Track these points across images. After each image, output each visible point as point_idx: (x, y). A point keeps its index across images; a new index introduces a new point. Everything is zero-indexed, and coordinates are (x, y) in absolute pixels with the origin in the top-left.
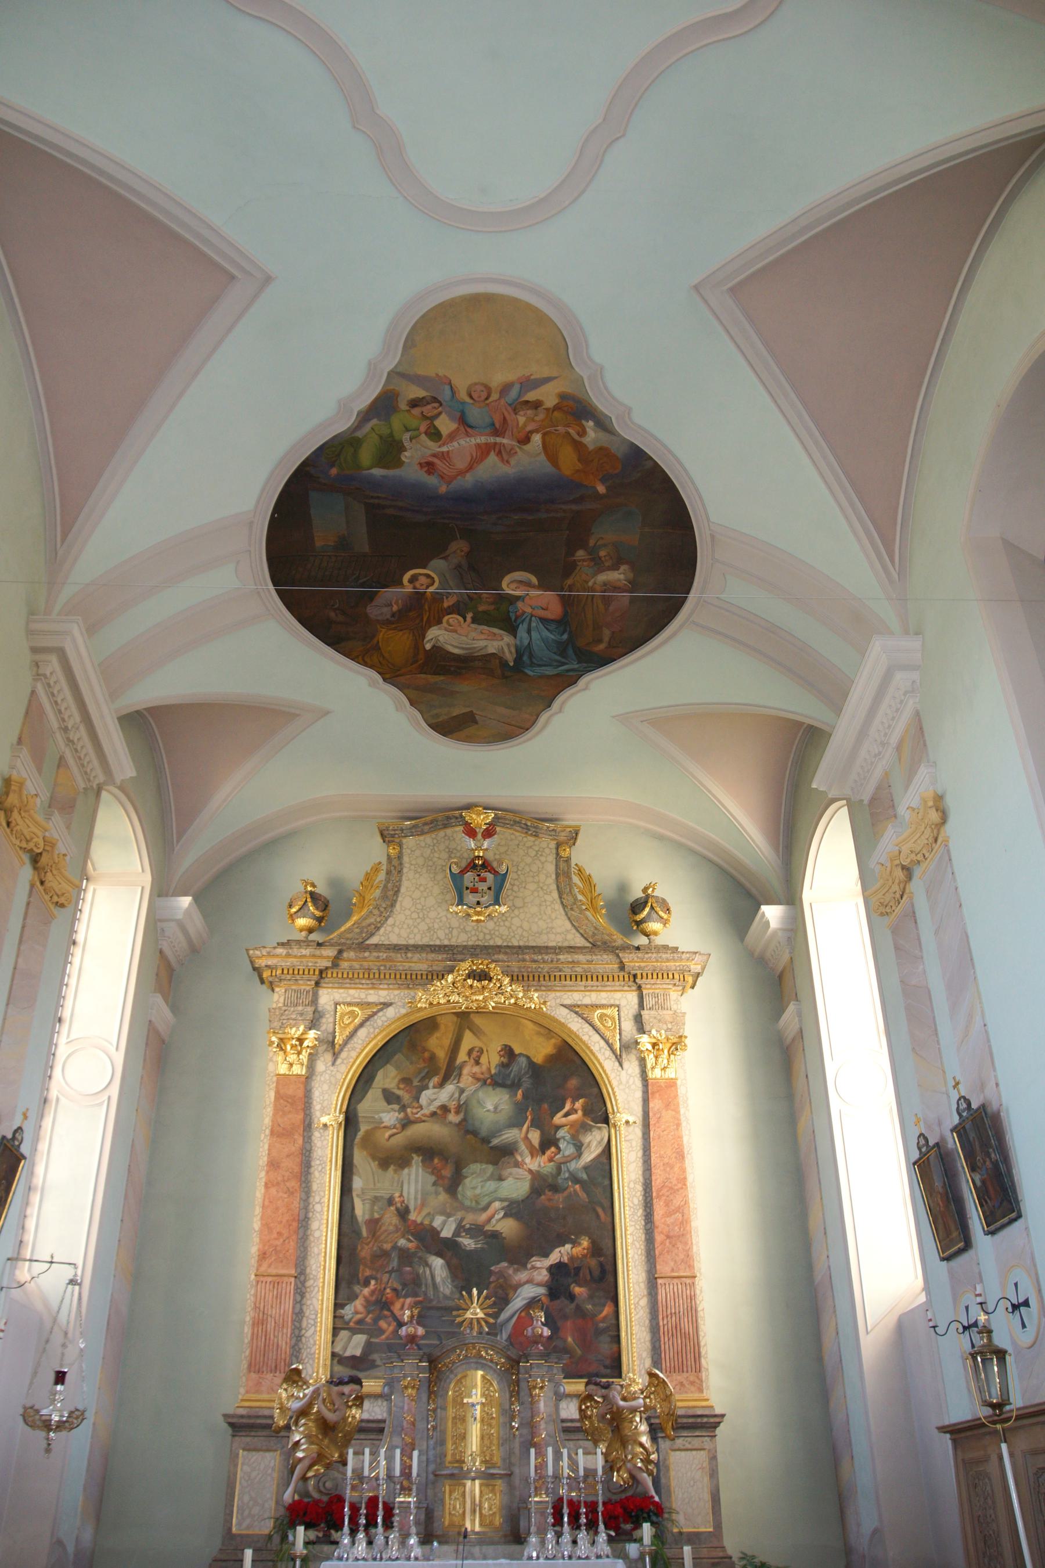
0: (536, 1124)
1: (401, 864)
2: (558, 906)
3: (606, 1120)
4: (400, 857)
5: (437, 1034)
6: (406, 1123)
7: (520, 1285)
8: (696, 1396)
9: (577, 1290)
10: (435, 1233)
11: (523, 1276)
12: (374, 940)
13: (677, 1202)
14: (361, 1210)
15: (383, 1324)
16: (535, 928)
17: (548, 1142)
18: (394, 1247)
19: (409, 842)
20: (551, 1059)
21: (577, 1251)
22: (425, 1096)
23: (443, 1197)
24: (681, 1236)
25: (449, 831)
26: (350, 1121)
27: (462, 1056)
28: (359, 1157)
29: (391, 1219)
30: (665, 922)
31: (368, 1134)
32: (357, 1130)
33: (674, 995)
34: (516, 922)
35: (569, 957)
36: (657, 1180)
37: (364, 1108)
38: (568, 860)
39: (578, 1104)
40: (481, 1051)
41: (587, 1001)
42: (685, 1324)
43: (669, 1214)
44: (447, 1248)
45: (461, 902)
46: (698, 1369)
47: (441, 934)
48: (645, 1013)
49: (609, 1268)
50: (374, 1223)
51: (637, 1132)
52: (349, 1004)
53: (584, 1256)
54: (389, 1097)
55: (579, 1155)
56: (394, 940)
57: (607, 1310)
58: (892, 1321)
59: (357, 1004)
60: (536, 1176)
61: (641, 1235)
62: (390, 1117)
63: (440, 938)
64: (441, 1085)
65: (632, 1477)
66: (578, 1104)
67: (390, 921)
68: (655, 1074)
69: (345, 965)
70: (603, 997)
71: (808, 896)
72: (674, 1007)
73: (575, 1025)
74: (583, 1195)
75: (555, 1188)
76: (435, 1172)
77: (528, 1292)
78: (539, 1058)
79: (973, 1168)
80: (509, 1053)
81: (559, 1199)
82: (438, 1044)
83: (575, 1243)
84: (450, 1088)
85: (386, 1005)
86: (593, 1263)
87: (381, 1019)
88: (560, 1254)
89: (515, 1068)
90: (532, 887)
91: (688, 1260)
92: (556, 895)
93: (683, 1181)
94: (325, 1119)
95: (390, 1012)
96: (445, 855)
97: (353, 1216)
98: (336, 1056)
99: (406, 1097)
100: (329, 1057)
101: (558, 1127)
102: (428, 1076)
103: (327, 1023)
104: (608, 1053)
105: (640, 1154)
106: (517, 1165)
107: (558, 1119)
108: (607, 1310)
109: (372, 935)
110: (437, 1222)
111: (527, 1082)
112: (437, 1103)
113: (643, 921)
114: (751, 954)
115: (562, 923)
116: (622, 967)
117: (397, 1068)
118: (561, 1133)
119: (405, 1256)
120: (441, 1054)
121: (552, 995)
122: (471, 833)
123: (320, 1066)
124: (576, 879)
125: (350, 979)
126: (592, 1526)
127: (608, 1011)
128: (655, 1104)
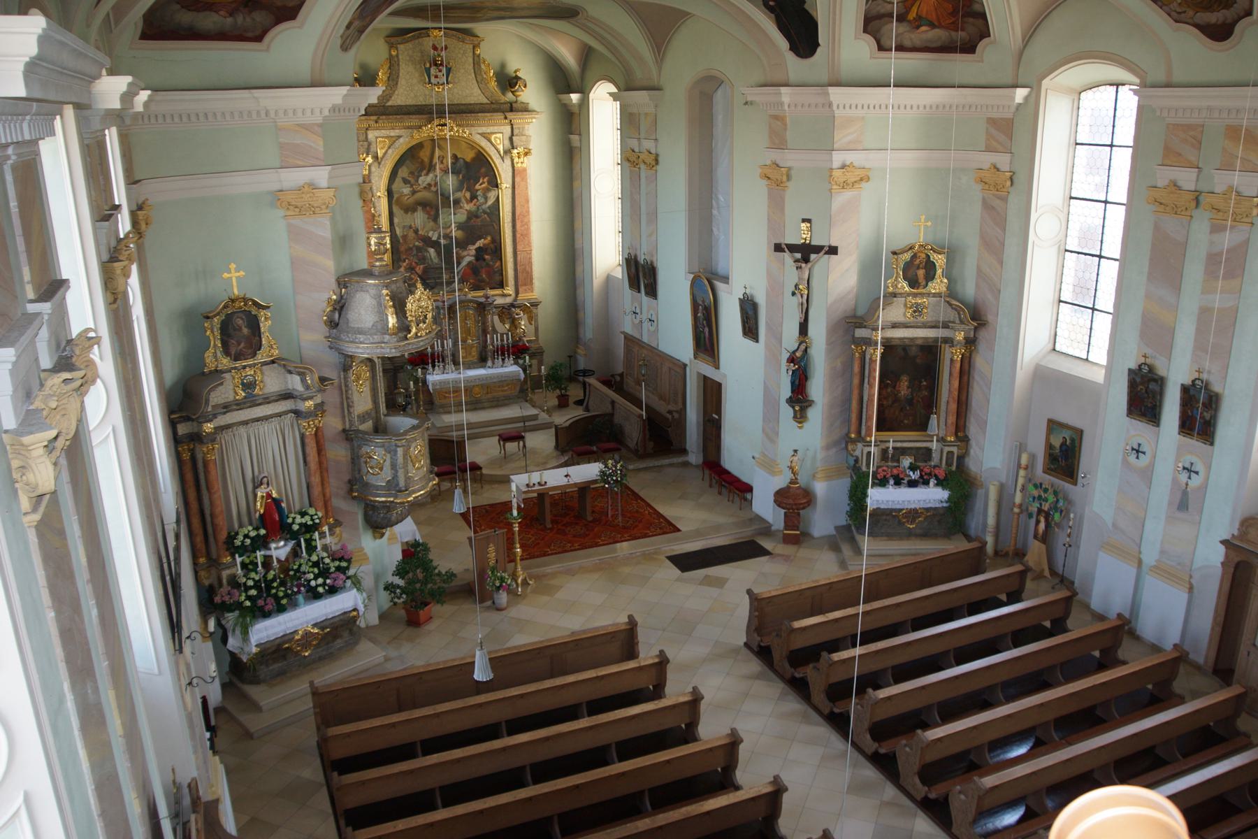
0: (467, 190)
1: (398, 60)
2: (475, 81)
3: (497, 187)
4: (397, 56)
5: (423, 150)
6: (414, 192)
7: (465, 256)
8: (531, 294)
9: (486, 257)
10: (430, 238)
11: (465, 253)
12: (390, 103)
13: (526, 220)
14: (398, 232)
15: (413, 276)
16: (464, 94)
17: (474, 197)
18: (414, 246)
19: (401, 47)
20: (474, 159)
21: (486, 242)
22: (421, 179)
23: (432, 224)
24: (527, 235)
25: (420, 40)
26: (390, 193)
27: (436, 160)
28: (395, 209)
29: (411, 234)
30: (523, 91)
31: (398, 199)
32: (393, 197)
33: (526, 126)
34: (456, 91)
35: (483, 114)
36: (517, 214)
37: (395, 187)
38: (479, 56)
39: (486, 180)
40: (443, 157)
41: (489, 131)
42: (528, 268)
43: (521, 226)
44: (436, 244)
45: (430, 82)
46: (531, 283)
47: (421, 99)
48: (514, 138)
49: (498, 248)
50: (405, 237)
51: (510, 191)
52: (382, 137)
53: (488, 244)
54: (405, 181)
55: (486, 202)
56: (399, 102)
57: (498, 264)
58: (605, 275)
59: (386, 137)
60: (469, 212)
61: (511, 234)
62: (407, 190)
63: (421, 101)
64: (427, 174)
65: (520, 339)
66: (486, 180)
67: (396, 92)
68: (518, 166)
69: (381, 121)
70: (495, 129)
71: (592, 95)
72: (527, 133)
73: (484, 143)
74: (488, 219)
75: (477, 217)
76: (428, 213)
77: (468, 259)
78: (468, 160)
79: (645, 277)
80: (455, 157)
81: (479, 220)
82: (424, 155)
83: (485, 239)
84: (431, 175)
85: (399, 137)
86: (492, 246)
87: (397, 144)
88: (480, 243)
89: (458, 165)
90: (462, 71)
91: (529, 244)
92: (473, 75)
93: (528, 212)
94: (379, 194)
95: (401, 140)
96: (419, 54)
97: (396, 235)
98: (379, 164)
99: (412, 181)
100: (376, 164)
101: (477, 190)
102: (421, 171)
103: (373, 149)
104: (498, 156)
105: (511, 200)
106: (461, 208)
107: (477, 187)
108: (498, 264)
109: (388, 100)
110: (430, 234)
111: (464, 172)
112: (426, 183)
113: (515, 91)
114: (560, 100)
115: (477, 91)
116: (506, 118)
117: (408, 167)
118: (479, 193)
119: (419, 249)
120: (426, 160)
121: (473, 128)
122: (435, 48)
123: (373, 169)
124: (483, 66)
125: (383, 128)
126: (509, 357)
127: (498, 135)
128: (517, 179)
